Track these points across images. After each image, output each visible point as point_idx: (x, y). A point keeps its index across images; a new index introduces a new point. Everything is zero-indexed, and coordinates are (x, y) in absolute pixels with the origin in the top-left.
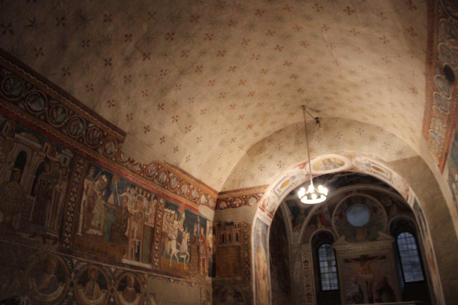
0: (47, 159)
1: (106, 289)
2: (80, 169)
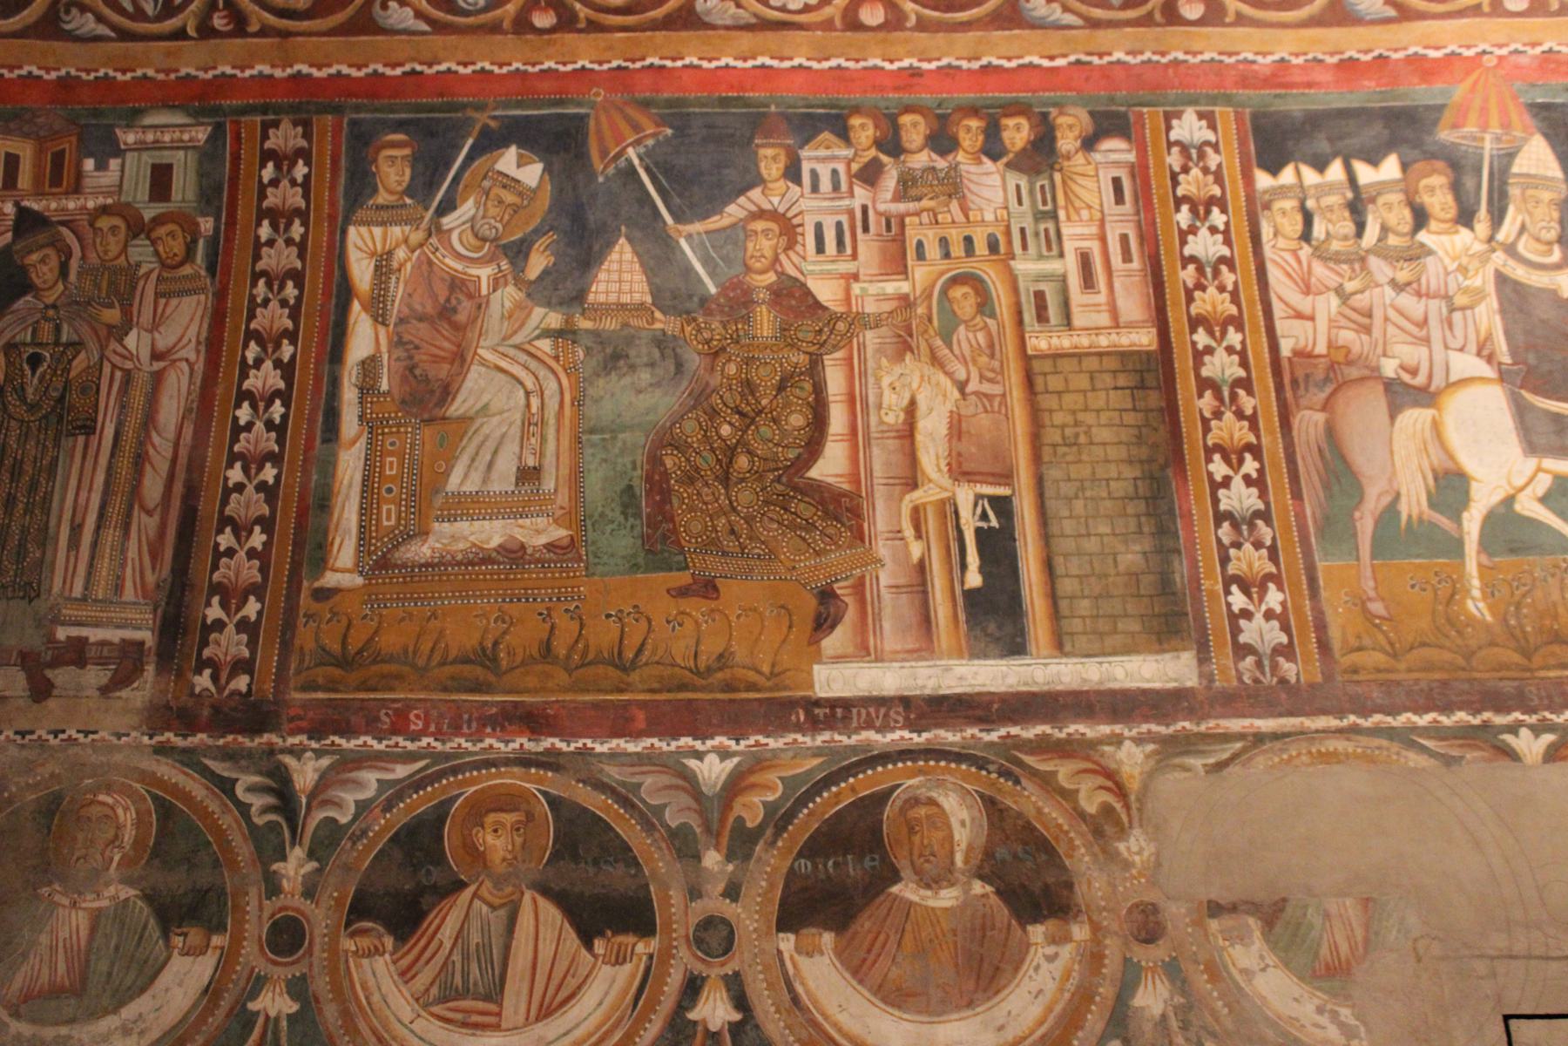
0: (27, 222)
1: (645, 927)
2: (293, 183)
